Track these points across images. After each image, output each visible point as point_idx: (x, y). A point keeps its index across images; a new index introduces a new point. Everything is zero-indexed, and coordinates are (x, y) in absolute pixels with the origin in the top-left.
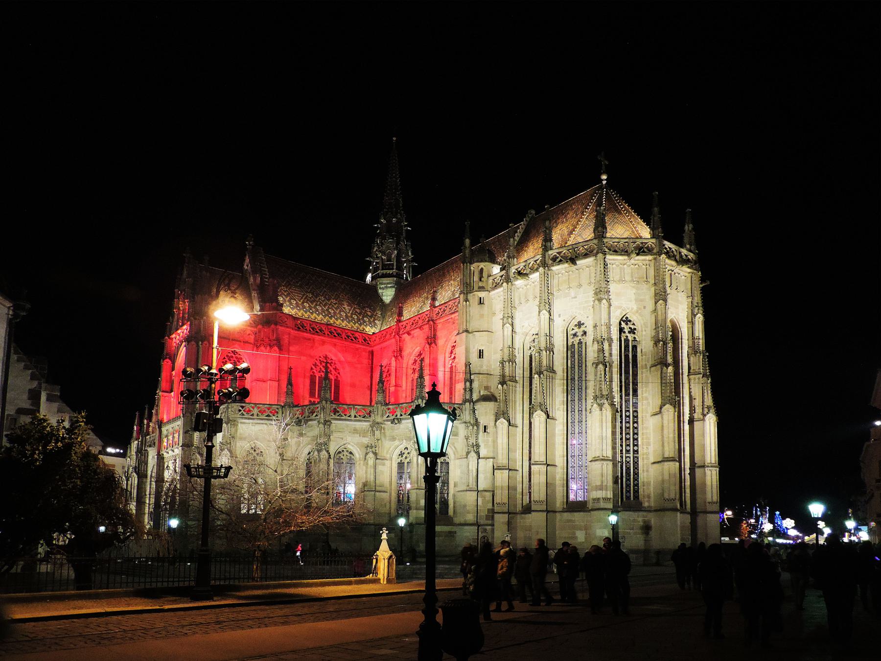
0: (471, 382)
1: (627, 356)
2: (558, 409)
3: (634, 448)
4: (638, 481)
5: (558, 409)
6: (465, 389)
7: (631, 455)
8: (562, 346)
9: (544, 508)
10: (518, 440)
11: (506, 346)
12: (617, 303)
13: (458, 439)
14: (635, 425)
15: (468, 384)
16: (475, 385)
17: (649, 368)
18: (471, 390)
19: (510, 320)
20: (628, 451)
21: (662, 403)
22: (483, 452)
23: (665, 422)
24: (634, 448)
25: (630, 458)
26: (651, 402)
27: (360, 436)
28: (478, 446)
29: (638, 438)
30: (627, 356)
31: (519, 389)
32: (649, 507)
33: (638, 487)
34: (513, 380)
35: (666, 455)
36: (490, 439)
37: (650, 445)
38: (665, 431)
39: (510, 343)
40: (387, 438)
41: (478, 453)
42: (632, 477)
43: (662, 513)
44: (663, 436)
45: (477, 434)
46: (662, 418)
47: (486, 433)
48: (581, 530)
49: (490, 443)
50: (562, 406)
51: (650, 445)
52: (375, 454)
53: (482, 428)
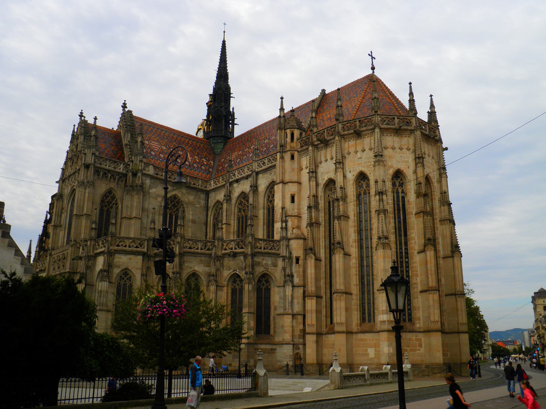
0: (286, 222)
1: (398, 205)
2: (352, 246)
4: (411, 306)
5: (352, 246)
6: (282, 228)
8: (353, 196)
9: (344, 329)
10: (322, 271)
11: (312, 194)
14: (407, 260)
15: (284, 224)
16: (290, 224)
17: (414, 215)
18: (286, 228)
19: (314, 174)
21: (425, 243)
22: (296, 280)
23: (428, 258)
26: (417, 242)
27: (204, 266)
28: (292, 276)
29: (409, 270)
31: (322, 229)
32: (420, 328)
33: (411, 311)
34: (318, 224)
35: (430, 285)
36: (301, 270)
37: (418, 277)
38: (429, 266)
39: (315, 192)
40: (225, 268)
41: (292, 282)
43: (428, 334)
44: (427, 270)
45: (291, 266)
46: (426, 255)
47: (298, 265)
48: (371, 347)
49: (301, 273)
50: (354, 244)
51: (418, 277)
52: (216, 281)
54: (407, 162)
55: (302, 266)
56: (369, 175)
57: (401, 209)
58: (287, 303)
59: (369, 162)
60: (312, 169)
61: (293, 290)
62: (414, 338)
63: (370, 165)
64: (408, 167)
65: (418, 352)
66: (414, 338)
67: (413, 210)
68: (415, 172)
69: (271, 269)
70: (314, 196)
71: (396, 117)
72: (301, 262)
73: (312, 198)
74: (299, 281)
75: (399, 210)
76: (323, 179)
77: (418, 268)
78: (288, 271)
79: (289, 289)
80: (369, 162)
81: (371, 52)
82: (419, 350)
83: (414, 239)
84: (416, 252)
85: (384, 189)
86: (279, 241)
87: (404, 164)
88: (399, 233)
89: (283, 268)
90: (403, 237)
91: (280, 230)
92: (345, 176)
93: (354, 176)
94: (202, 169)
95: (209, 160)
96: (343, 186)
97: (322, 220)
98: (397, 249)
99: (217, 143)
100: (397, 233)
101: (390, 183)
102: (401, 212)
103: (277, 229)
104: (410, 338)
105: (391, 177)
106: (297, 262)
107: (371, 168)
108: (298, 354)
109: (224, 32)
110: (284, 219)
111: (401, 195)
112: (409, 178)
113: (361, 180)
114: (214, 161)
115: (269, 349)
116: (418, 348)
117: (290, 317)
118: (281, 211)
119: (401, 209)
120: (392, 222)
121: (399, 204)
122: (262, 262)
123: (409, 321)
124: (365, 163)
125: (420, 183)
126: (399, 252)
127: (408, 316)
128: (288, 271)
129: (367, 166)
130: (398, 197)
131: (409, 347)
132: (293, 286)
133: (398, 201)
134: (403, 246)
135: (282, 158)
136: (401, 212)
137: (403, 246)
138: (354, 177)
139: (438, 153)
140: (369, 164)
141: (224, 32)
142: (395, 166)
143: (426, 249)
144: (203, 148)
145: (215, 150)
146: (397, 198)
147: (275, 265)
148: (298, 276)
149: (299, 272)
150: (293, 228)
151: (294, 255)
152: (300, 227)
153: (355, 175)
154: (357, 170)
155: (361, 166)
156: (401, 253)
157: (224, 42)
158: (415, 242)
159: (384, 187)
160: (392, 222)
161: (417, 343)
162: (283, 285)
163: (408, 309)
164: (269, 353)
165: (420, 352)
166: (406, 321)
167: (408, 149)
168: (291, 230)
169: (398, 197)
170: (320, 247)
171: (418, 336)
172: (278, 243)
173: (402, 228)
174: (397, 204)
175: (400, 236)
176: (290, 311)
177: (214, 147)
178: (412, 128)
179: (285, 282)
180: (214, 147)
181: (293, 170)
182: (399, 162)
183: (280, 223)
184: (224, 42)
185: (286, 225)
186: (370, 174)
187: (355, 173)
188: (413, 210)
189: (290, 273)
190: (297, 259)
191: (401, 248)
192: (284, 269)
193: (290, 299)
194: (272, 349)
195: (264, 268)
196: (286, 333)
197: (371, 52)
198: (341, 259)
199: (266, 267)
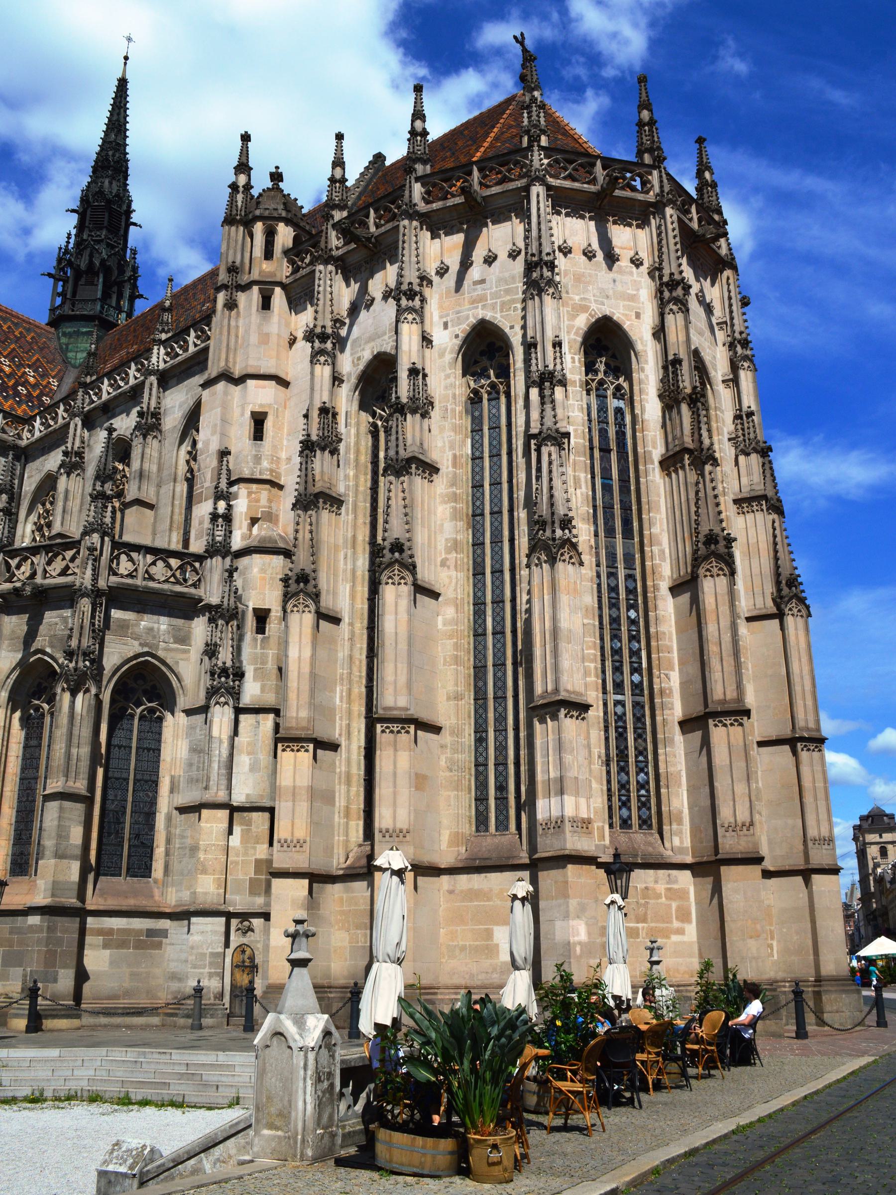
1: (603, 433)
3: (633, 678)
6: (214, 517)
7: (628, 698)
11: (318, 404)
12: (577, 298)
13: (188, 651)
15: (222, 505)
18: (228, 518)
20: (619, 687)
24: (633, 678)
25: (624, 706)
28: (240, 675)
30: (603, 433)
36: (271, 653)
41: (235, 694)
42: (632, 759)
45: (239, 639)
47: (260, 636)
49: (271, 666)
53: (250, 622)
54: (633, 298)
55: (273, 642)
56: (507, 330)
57: (613, 446)
58: (215, 766)
59: (508, 292)
60: (324, 327)
61: (236, 722)
62: (661, 888)
63: (513, 301)
64: (638, 315)
65: (675, 938)
66: (661, 888)
67: (654, 447)
68: (660, 333)
69: (167, 651)
70: (324, 411)
71: (599, 163)
72: (273, 626)
73: (315, 414)
74: (263, 690)
75: (605, 451)
76: (359, 359)
77: (671, 640)
78: (225, 656)
79: (222, 716)
80: (508, 292)
81: (522, 34)
82: (681, 932)
83: (660, 544)
84: (664, 586)
85: (559, 367)
86: (200, 558)
87: (622, 303)
88: (606, 524)
89: (207, 645)
90: (619, 536)
91: (207, 524)
92: (426, 340)
93: (457, 336)
94: (17, 394)
95: (44, 375)
96: (419, 367)
97: (347, 488)
98: (599, 576)
99: (78, 333)
100: (601, 521)
101: (577, 357)
102: (614, 456)
103: (201, 523)
104: (647, 888)
105: (580, 339)
106: (261, 629)
107: (515, 309)
108: (243, 952)
109: (126, 58)
110: (223, 485)
111: (613, 403)
112: (639, 347)
113: (482, 353)
114: (60, 381)
115: (138, 932)
116: (676, 924)
117: (224, 814)
118: (214, 463)
119: (613, 446)
120: (583, 480)
121: (606, 431)
122: (138, 625)
123: (640, 827)
124: (495, 295)
125: (677, 362)
126: (604, 587)
127: (639, 809)
128: (225, 656)
129: (503, 304)
130: (602, 409)
131: (644, 921)
132: (239, 711)
133: (603, 421)
134: (621, 565)
135: (231, 305)
136: (614, 456)
137: (621, 565)
138: (458, 342)
139: (726, 295)
140: (508, 298)
141: (126, 58)
142: (594, 306)
143: (701, 572)
144: (30, 344)
145: (70, 355)
146: (599, 412)
147: (183, 639)
148: (260, 674)
149: (264, 662)
150: (254, 521)
151: (253, 601)
152: (277, 516)
153: (462, 335)
154: (468, 317)
155: (484, 307)
156: (614, 589)
157: (123, 84)
158: (662, 552)
159: (558, 361)
160: (583, 480)
161: (674, 905)
162: (201, 702)
163: (638, 782)
164: (139, 945)
165: (685, 938)
166: (630, 827)
167: (637, 262)
168: (246, 523)
169: (602, 409)
170: (335, 575)
171: (676, 882)
172: (197, 565)
173: (617, 506)
174: (600, 431)
175: (610, 532)
176: (222, 796)
177: (67, 345)
178: (651, 197)
179: (212, 692)
180: (67, 345)
181: (265, 339)
182: (608, 297)
183: (210, 503)
184: (123, 84)
185: (229, 507)
186: (512, 327)
187: (463, 328)
188: (654, 447)
189: (229, 664)
190: (262, 616)
191: (612, 575)
192: (211, 651)
193: (225, 753)
194: (151, 933)
195: (141, 644)
196: (204, 871)
197: (522, 34)
198: (404, 603)
199: (150, 640)
